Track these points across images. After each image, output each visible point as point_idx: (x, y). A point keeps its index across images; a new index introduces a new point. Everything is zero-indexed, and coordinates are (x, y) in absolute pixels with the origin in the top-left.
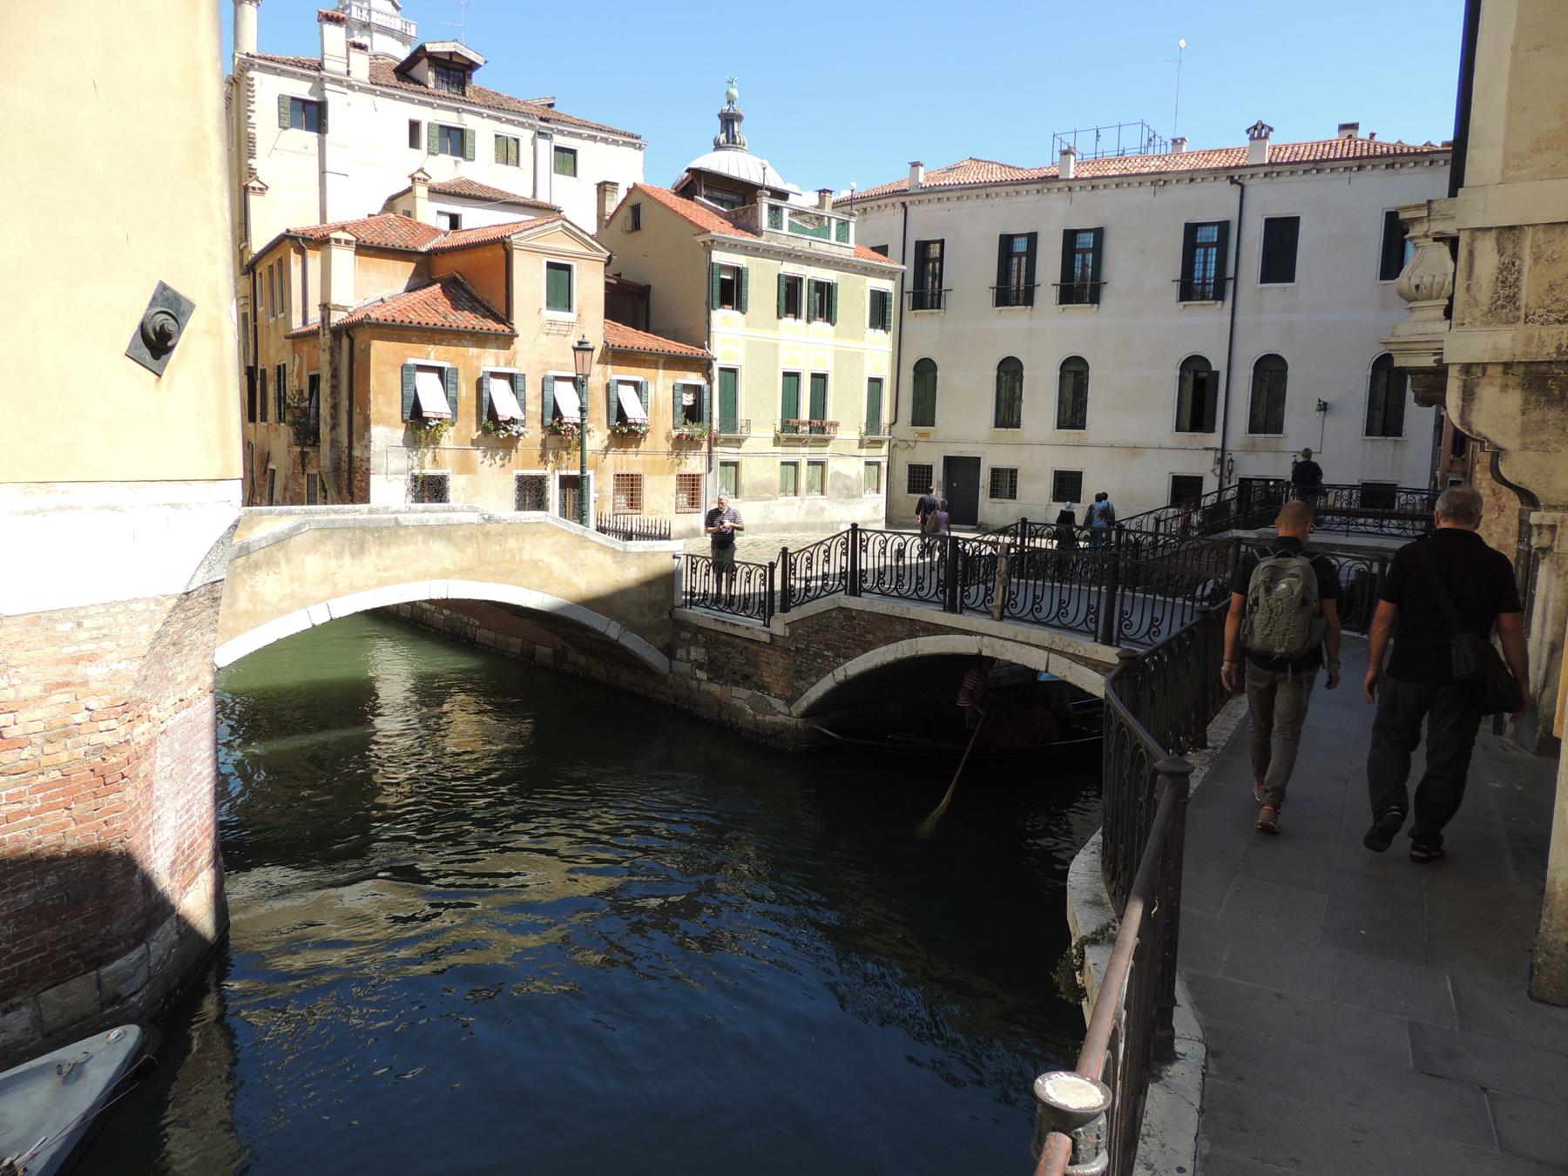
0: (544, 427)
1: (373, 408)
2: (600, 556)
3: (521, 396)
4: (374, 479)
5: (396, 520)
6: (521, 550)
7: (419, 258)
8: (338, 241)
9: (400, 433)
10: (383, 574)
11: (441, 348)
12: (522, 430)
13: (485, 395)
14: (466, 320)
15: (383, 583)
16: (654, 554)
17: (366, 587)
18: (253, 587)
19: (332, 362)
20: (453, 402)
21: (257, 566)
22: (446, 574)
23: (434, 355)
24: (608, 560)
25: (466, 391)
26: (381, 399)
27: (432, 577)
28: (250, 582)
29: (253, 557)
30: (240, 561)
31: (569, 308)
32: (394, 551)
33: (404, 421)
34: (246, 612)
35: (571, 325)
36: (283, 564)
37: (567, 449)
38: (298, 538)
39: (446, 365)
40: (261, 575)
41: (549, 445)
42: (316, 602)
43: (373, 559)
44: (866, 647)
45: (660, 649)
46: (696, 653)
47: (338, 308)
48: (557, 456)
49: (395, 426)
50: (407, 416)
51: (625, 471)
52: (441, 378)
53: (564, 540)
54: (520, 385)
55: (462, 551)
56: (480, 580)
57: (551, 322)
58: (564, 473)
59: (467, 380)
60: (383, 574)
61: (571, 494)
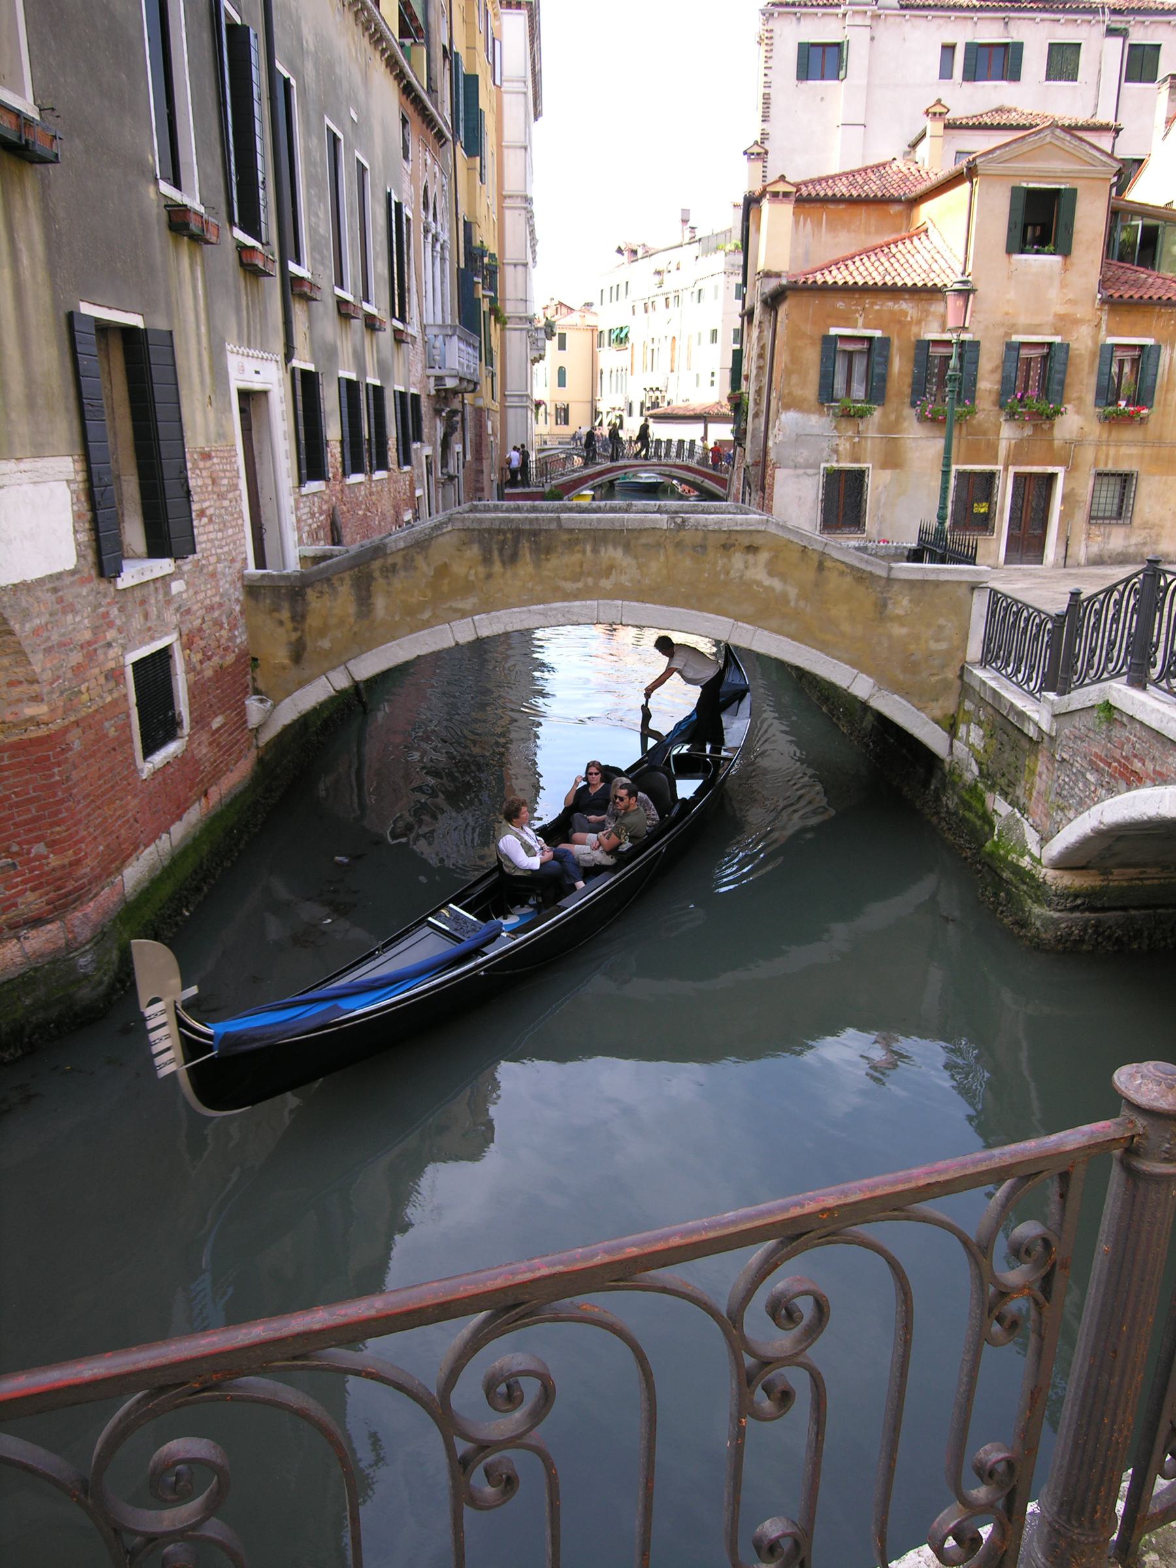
8: (775, 195)
19: (759, 339)
38: (441, 539)
39: (878, 334)
44: (1132, 779)
51: (1110, 468)
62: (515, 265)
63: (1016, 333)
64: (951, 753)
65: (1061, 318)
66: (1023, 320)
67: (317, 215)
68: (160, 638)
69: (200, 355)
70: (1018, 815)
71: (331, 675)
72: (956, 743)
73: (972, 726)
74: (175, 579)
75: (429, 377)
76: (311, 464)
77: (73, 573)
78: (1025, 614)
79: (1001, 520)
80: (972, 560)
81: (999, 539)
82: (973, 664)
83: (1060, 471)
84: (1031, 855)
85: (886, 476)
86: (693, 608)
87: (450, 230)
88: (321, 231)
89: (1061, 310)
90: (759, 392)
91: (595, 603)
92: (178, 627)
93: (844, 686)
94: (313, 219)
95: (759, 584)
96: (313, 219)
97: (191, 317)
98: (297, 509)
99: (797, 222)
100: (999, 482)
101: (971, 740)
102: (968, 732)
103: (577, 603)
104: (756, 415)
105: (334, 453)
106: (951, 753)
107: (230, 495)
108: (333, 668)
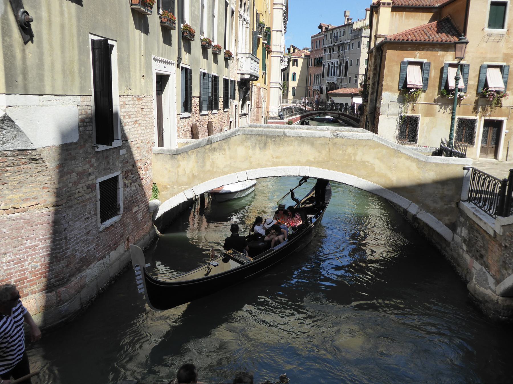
0: (478, 93)
1: (384, 83)
2: (408, 163)
3: (466, 76)
4: (381, 118)
5: (284, 133)
6: (355, 154)
7: (435, 10)
9: (396, 95)
10: (275, 160)
11: (423, 53)
12: (462, 94)
13: (444, 76)
14: (444, 37)
15: (275, 164)
16: (448, 165)
17: (266, 166)
18: (213, 159)
19: (375, 62)
20: (426, 80)
21: (215, 150)
22: (309, 163)
23: (418, 56)
24: (414, 166)
25: (434, 74)
26: (389, 79)
27: (302, 164)
28: (211, 157)
29: (214, 145)
30: (208, 147)
31: (503, 28)
32: (282, 149)
33: (399, 90)
34: (209, 171)
35: (502, 36)
36: (227, 150)
37: (491, 105)
38: (235, 137)
39: (425, 61)
40: (217, 154)
41: (480, 103)
42: (241, 170)
43: (271, 151)
45: (447, 225)
46: (464, 232)
47: (380, 36)
48: (484, 109)
49: (394, 92)
50: (400, 87)
52: (421, 68)
53: (384, 151)
54: (466, 71)
55: (319, 152)
56: (329, 169)
57: (490, 35)
58: (487, 118)
59: (435, 68)
60: (275, 160)
61: (492, 131)
62: (277, 31)
63: (486, 61)
64: (453, 240)
65: (506, 55)
66: (489, 56)
67: (195, 7)
68: (113, 173)
69: (140, 59)
70: (485, 270)
71: (185, 192)
72: (456, 236)
73: (463, 229)
74: (122, 149)
75: (238, 74)
76: (187, 106)
77: (76, 143)
78: (488, 180)
79: (478, 139)
80: (463, 156)
81: (477, 147)
82: (464, 201)
83: (505, 119)
84: (491, 289)
85: (427, 119)
86: (340, 171)
87: (250, 16)
88: (196, 13)
89: (506, 51)
90: (374, 84)
91: (298, 167)
92: (122, 169)
93: (405, 208)
94: (193, 8)
95: (368, 162)
96: (193, 8)
97: (138, 43)
98: (178, 123)
99: (393, 15)
100: (477, 124)
101: (463, 235)
102: (461, 231)
103: (291, 167)
104: (372, 94)
105: (195, 102)
106: (453, 240)
107: (149, 116)
108: (186, 189)
